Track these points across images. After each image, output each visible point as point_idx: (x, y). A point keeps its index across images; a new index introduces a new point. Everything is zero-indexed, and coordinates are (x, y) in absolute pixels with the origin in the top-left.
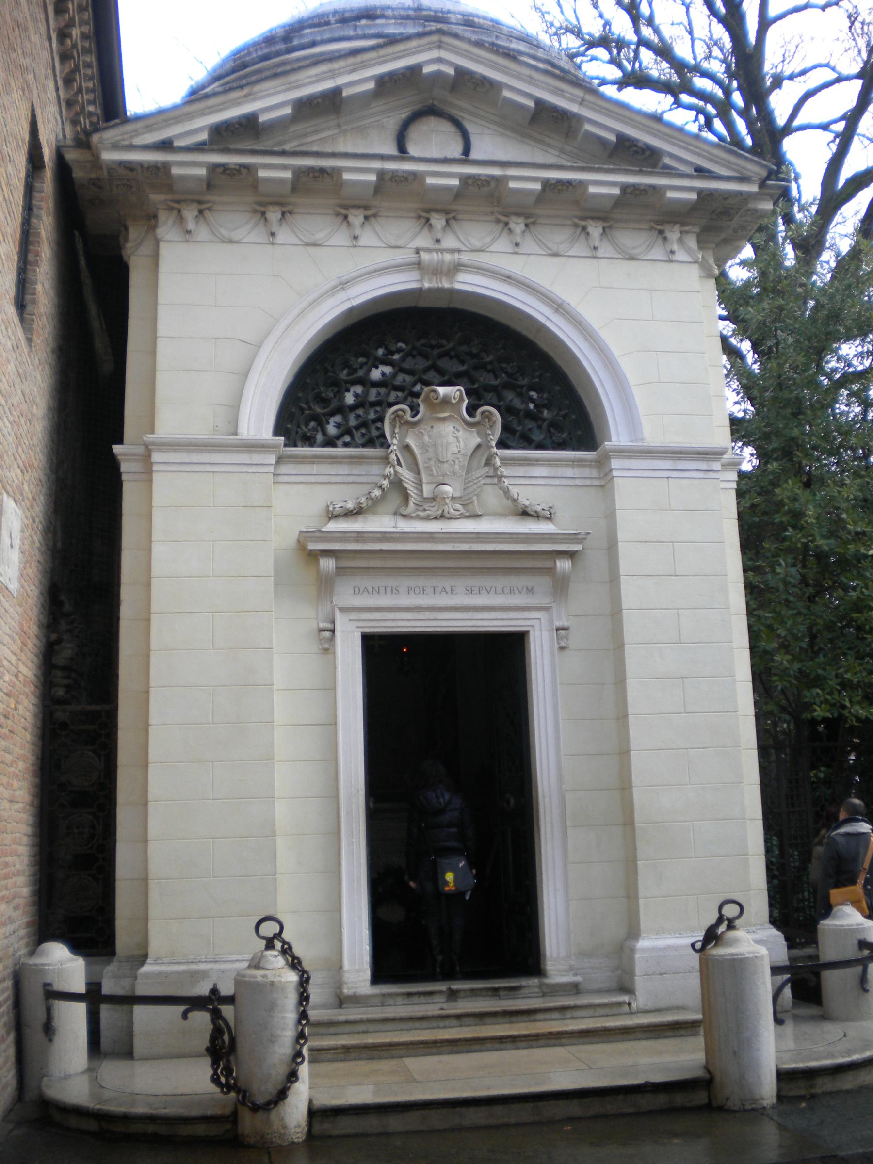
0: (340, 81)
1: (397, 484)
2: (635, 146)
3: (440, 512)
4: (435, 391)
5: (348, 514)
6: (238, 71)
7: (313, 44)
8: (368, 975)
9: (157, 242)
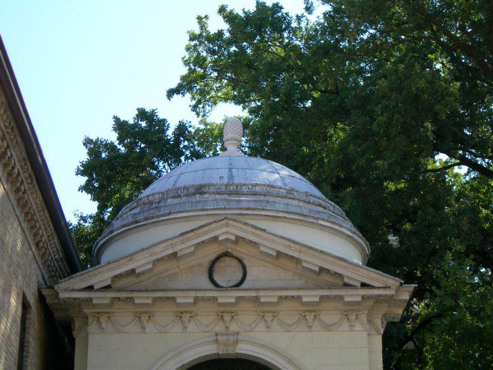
6: (133, 224)
7: (170, 213)
9: (87, 334)
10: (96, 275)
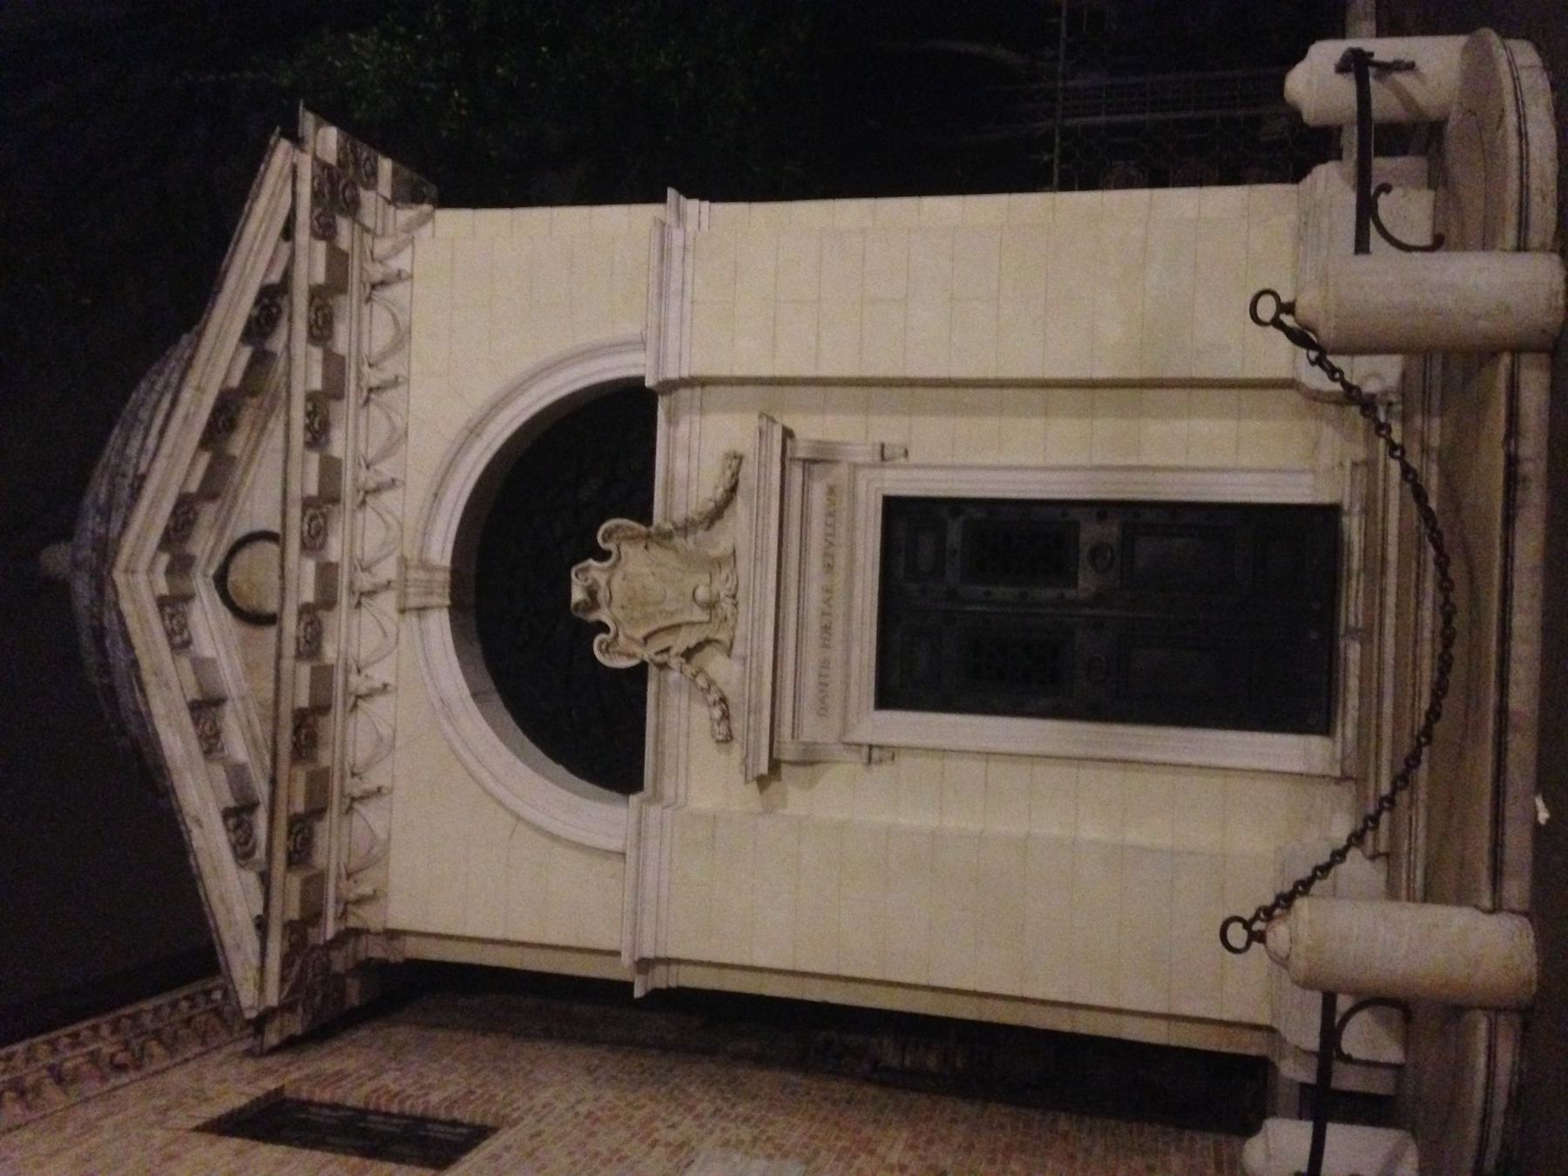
0: (183, 705)
1: (688, 654)
2: (257, 319)
3: (729, 600)
4: (577, 605)
5: (726, 716)
8: (1315, 743)
10: (229, 910)
